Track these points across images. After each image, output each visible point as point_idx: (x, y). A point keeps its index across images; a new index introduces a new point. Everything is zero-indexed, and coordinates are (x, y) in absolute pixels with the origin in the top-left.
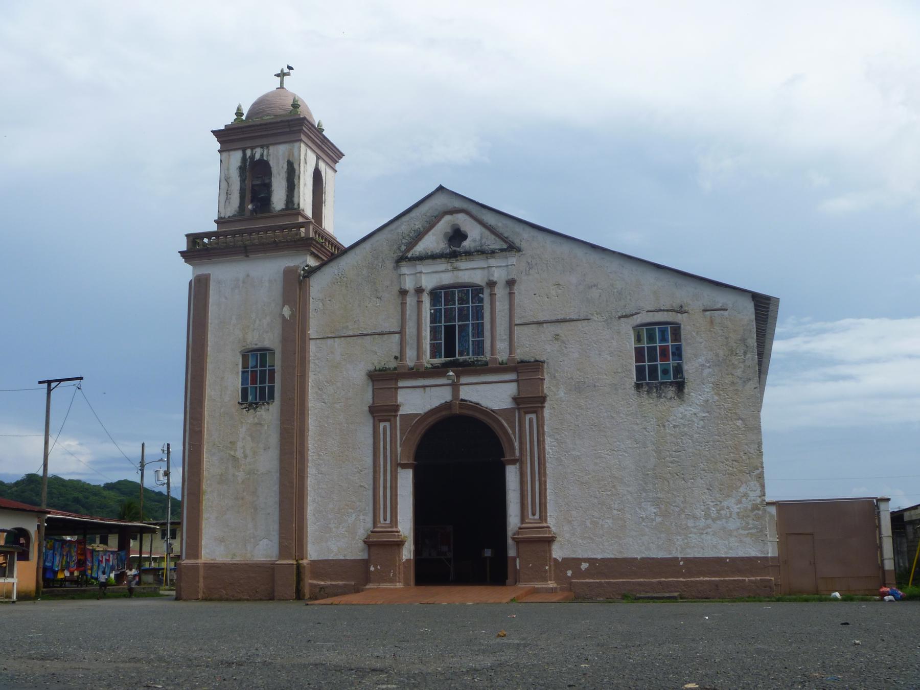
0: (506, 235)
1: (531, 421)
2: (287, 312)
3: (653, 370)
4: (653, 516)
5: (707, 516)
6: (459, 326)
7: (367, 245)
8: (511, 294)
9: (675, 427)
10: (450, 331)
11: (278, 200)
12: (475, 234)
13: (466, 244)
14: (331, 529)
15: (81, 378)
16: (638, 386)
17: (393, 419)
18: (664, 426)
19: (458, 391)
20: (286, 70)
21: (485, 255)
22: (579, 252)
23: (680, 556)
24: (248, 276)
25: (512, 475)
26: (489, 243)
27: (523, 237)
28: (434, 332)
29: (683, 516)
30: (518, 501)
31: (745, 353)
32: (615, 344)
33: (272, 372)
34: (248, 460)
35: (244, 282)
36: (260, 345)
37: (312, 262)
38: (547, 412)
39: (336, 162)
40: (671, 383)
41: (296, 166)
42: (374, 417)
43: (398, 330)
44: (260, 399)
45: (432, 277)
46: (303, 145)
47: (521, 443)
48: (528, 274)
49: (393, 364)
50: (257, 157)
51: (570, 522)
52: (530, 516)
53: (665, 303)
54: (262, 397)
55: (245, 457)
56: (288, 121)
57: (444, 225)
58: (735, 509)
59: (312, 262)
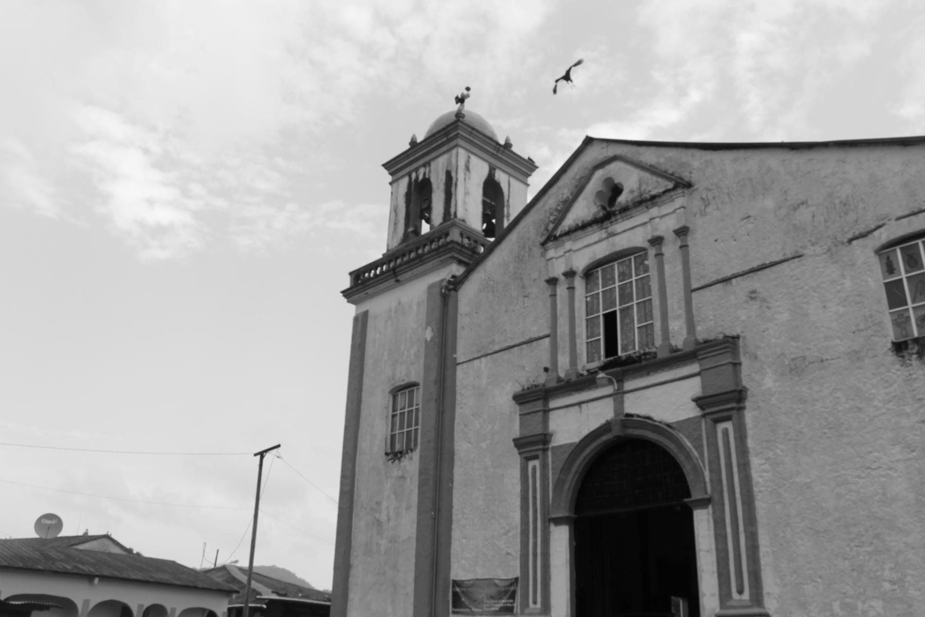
0: (670, 171)
1: (726, 433)
2: (429, 335)
8: (684, 247)
10: (610, 319)
13: (622, 199)
15: (279, 446)
17: (540, 453)
19: (622, 402)
20: (466, 92)
21: (644, 205)
24: (399, 303)
25: (703, 524)
26: (649, 188)
28: (591, 324)
32: (848, 283)
34: (391, 523)
35: (396, 312)
36: (407, 380)
37: (457, 270)
38: (749, 416)
39: (528, 175)
41: (453, 175)
43: (547, 331)
45: (585, 252)
46: (462, 152)
47: (715, 471)
48: (703, 214)
49: (542, 379)
50: (421, 177)
52: (735, 595)
55: (389, 520)
57: (595, 184)
59: (457, 270)
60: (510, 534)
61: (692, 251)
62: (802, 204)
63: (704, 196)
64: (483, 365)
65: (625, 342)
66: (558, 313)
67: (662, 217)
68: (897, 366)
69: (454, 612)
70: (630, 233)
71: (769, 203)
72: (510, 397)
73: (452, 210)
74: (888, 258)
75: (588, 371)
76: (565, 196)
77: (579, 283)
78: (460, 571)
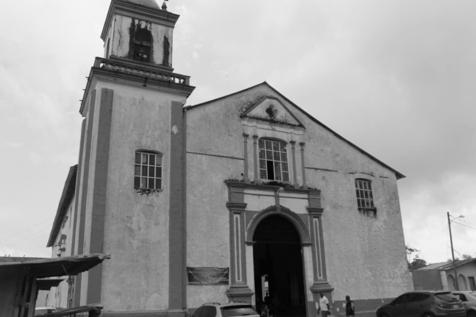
0: (298, 118)
4: (370, 277)
5: (390, 277)
6: (275, 162)
7: (223, 102)
8: (302, 150)
9: (375, 231)
10: (270, 164)
11: (158, 57)
12: (281, 114)
16: (360, 209)
17: (242, 212)
21: (289, 126)
22: (331, 136)
23: (382, 298)
25: (307, 253)
27: (306, 121)
28: (262, 162)
29: (381, 277)
30: (312, 267)
31: (396, 199)
33: (159, 170)
34: (141, 231)
35: (140, 102)
36: (151, 149)
38: (323, 218)
41: (170, 41)
42: (230, 210)
43: (243, 157)
49: (240, 178)
50: (143, 26)
52: (319, 277)
53: (366, 170)
55: (140, 229)
57: (266, 103)
58: (399, 273)
60: (223, 247)
64: (203, 159)
66: (248, 151)
67: (295, 134)
69: (190, 284)
70: (282, 133)
71: (329, 149)
72: (222, 181)
76: (251, 100)
78: (191, 263)
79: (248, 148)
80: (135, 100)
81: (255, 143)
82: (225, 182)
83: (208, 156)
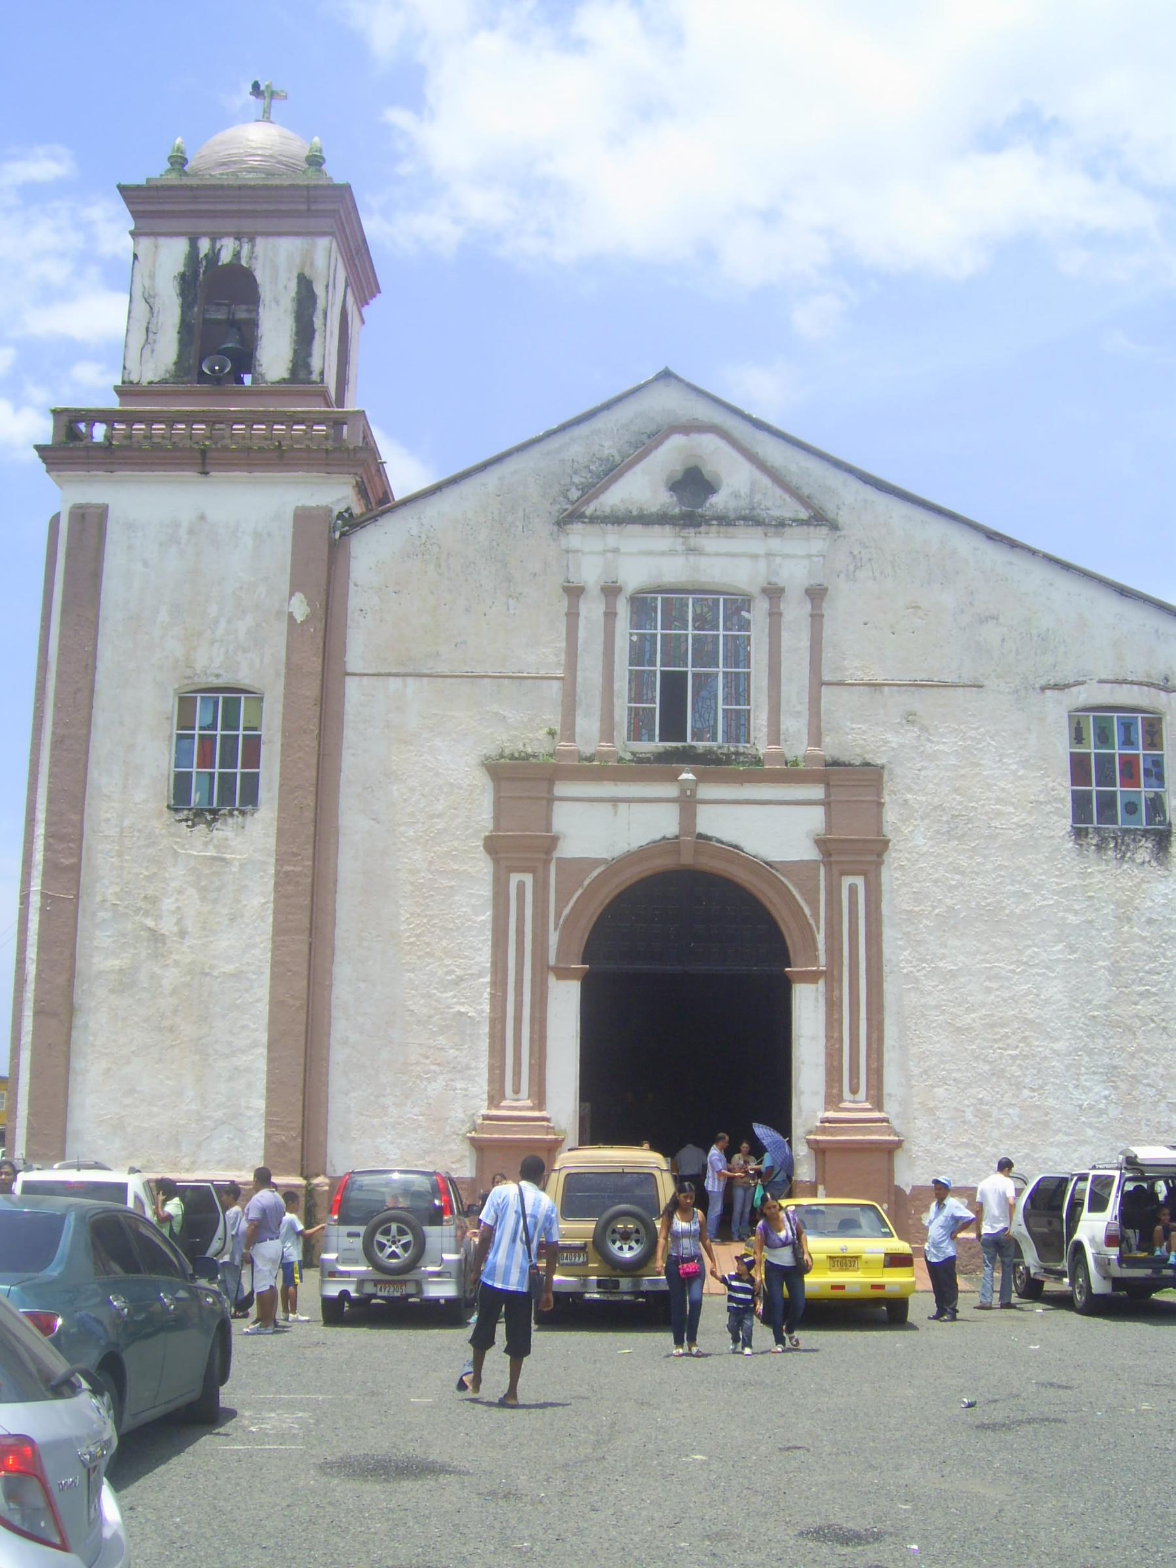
0: (805, 491)
1: (853, 889)
2: (299, 608)
3: (1107, 803)
6: (695, 675)
7: (491, 479)
8: (816, 618)
9: (1150, 922)
10: (674, 686)
11: (274, 354)
12: (735, 481)
13: (719, 501)
14: (384, 1108)
16: (1079, 834)
18: (1129, 919)
21: (760, 530)
22: (964, 543)
26: (769, 504)
28: (639, 684)
29: (1163, 1105)
35: (191, 532)
38: (889, 876)
40: (1145, 833)
41: (319, 289)
42: (496, 862)
44: (222, 802)
46: (334, 245)
50: (226, 257)
51: (931, 1111)
53: (1136, 667)
54: (227, 796)
55: (182, 934)
56: (308, 188)
57: (669, 456)
60: (464, 985)
61: (826, 621)
62: (992, 618)
63: (856, 552)
65: (699, 725)
67: (787, 556)
68: (1074, 855)
73: (316, 363)
74: (1078, 723)
75: (632, 753)
76: (607, 452)
77: (623, 609)
79: (582, 634)
80: (177, 525)
81: (610, 615)
82: (484, 765)
83: (425, 679)
